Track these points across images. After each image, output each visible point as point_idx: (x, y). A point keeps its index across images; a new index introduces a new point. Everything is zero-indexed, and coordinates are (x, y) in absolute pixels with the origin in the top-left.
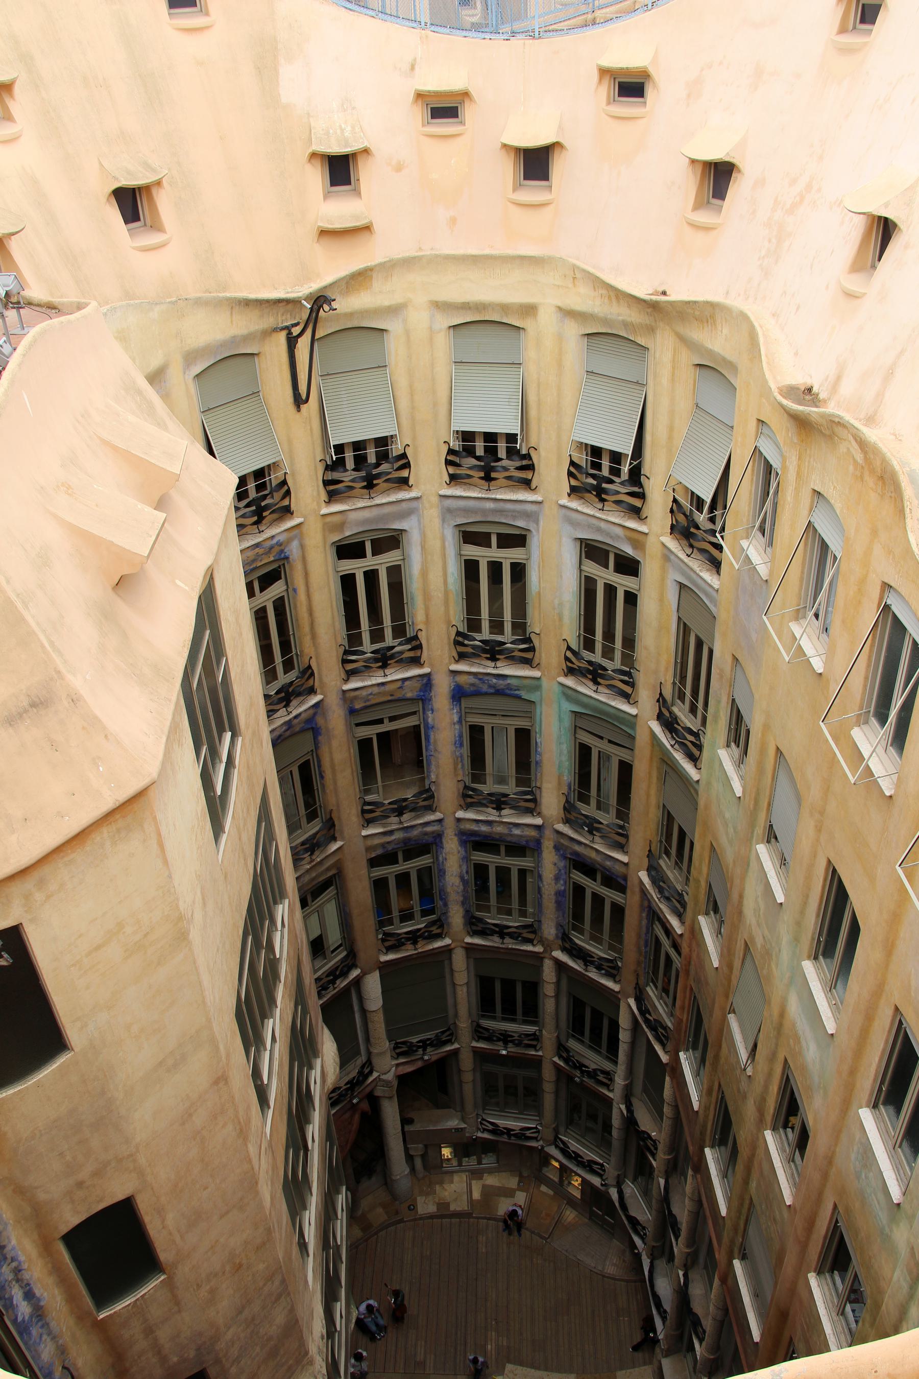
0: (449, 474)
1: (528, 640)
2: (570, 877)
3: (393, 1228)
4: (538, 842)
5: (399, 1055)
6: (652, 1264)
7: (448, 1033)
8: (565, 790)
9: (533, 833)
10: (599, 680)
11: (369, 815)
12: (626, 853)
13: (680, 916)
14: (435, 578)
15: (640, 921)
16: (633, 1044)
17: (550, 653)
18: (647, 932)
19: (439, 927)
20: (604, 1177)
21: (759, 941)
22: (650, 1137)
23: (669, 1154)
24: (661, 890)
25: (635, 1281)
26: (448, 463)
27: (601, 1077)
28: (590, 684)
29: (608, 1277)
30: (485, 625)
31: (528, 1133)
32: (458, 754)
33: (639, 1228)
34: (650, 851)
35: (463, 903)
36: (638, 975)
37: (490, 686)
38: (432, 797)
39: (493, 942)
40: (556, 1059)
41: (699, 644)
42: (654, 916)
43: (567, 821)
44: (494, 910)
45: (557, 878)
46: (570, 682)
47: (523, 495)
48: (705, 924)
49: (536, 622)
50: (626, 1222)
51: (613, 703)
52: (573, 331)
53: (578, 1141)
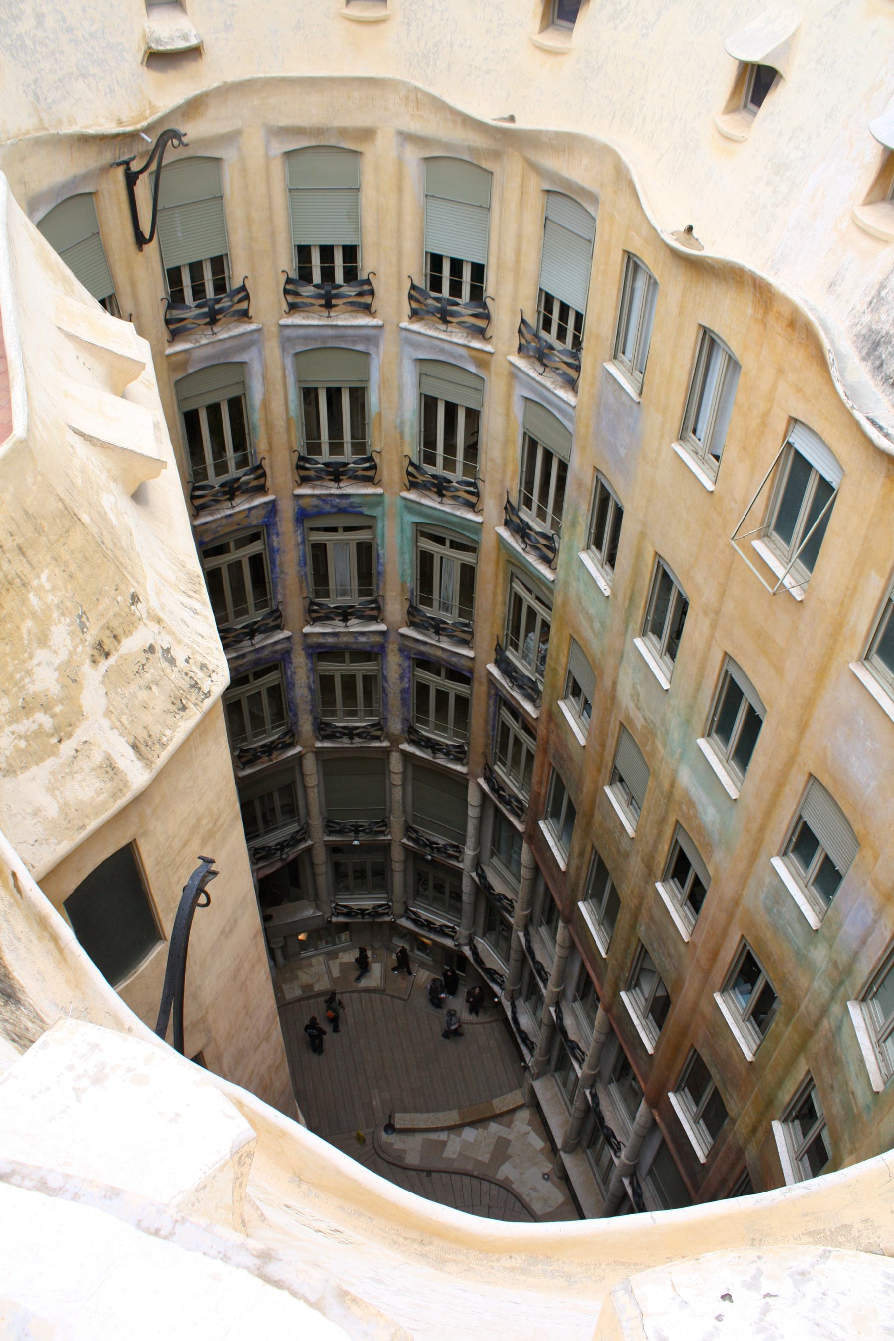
0: (288, 303)
1: (370, 459)
2: (414, 675)
4: (383, 647)
5: (258, 860)
6: (513, 1006)
8: (407, 595)
9: (378, 639)
10: (444, 492)
12: (471, 648)
13: (532, 700)
14: (277, 407)
15: (488, 708)
16: (481, 819)
17: (392, 470)
18: (494, 719)
21: (639, 722)
22: (506, 898)
23: (526, 910)
25: (490, 1022)
26: (286, 292)
28: (435, 497)
30: (325, 448)
31: (380, 910)
32: (303, 573)
33: (496, 976)
34: (498, 644)
35: (312, 712)
37: (333, 506)
39: (344, 743)
40: (405, 841)
41: (548, 456)
42: (503, 701)
43: (412, 624)
44: (340, 714)
45: (402, 678)
46: (412, 495)
47: (363, 320)
48: (568, 710)
49: (376, 441)
50: (483, 974)
51: (458, 513)
52: (412, 156)
53: (426, 910)
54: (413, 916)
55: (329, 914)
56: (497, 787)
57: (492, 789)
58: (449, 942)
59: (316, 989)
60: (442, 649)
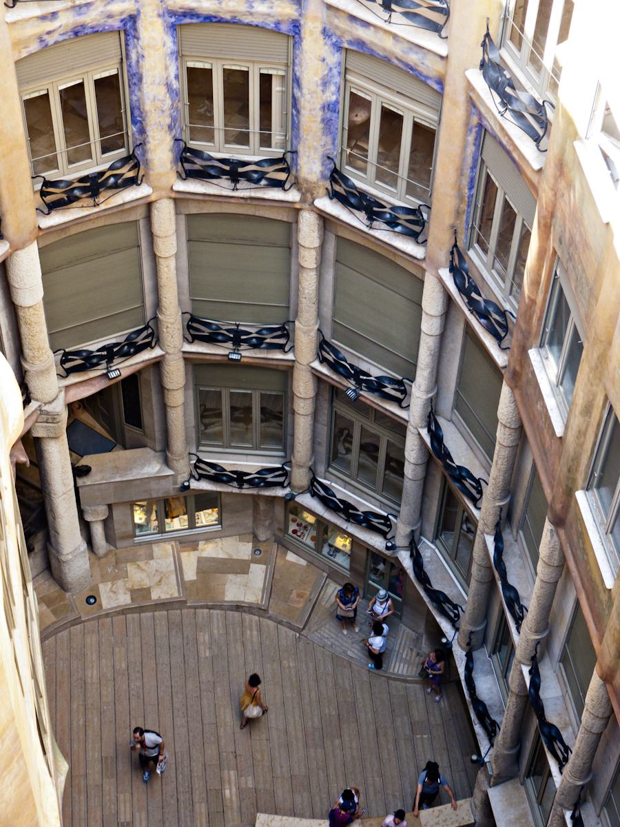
2: (346, 80)
3: (65, 633)
5: (69, 372)
6: (469, 657)
7: (145, 334)
16: (442, 338)
18: (473, 168)
19: (134, 166)
20: (389, 536)
23: (502, 499)
24: (507, 100)
27: (389, 390)
29: (395, 679)
33: (447, 607)
34: (487, 35)
35: (170, 128)
36: (455, 232)
39: (221, 187)
44: (219, 136)
45: (325, 84)
53: (346, 484)
54: (322, 493)
55: (186, 476)
56: (468, 286)
57: (461, 289)
58: (377, 542)
59: (155, 595)
60: (395, 36)
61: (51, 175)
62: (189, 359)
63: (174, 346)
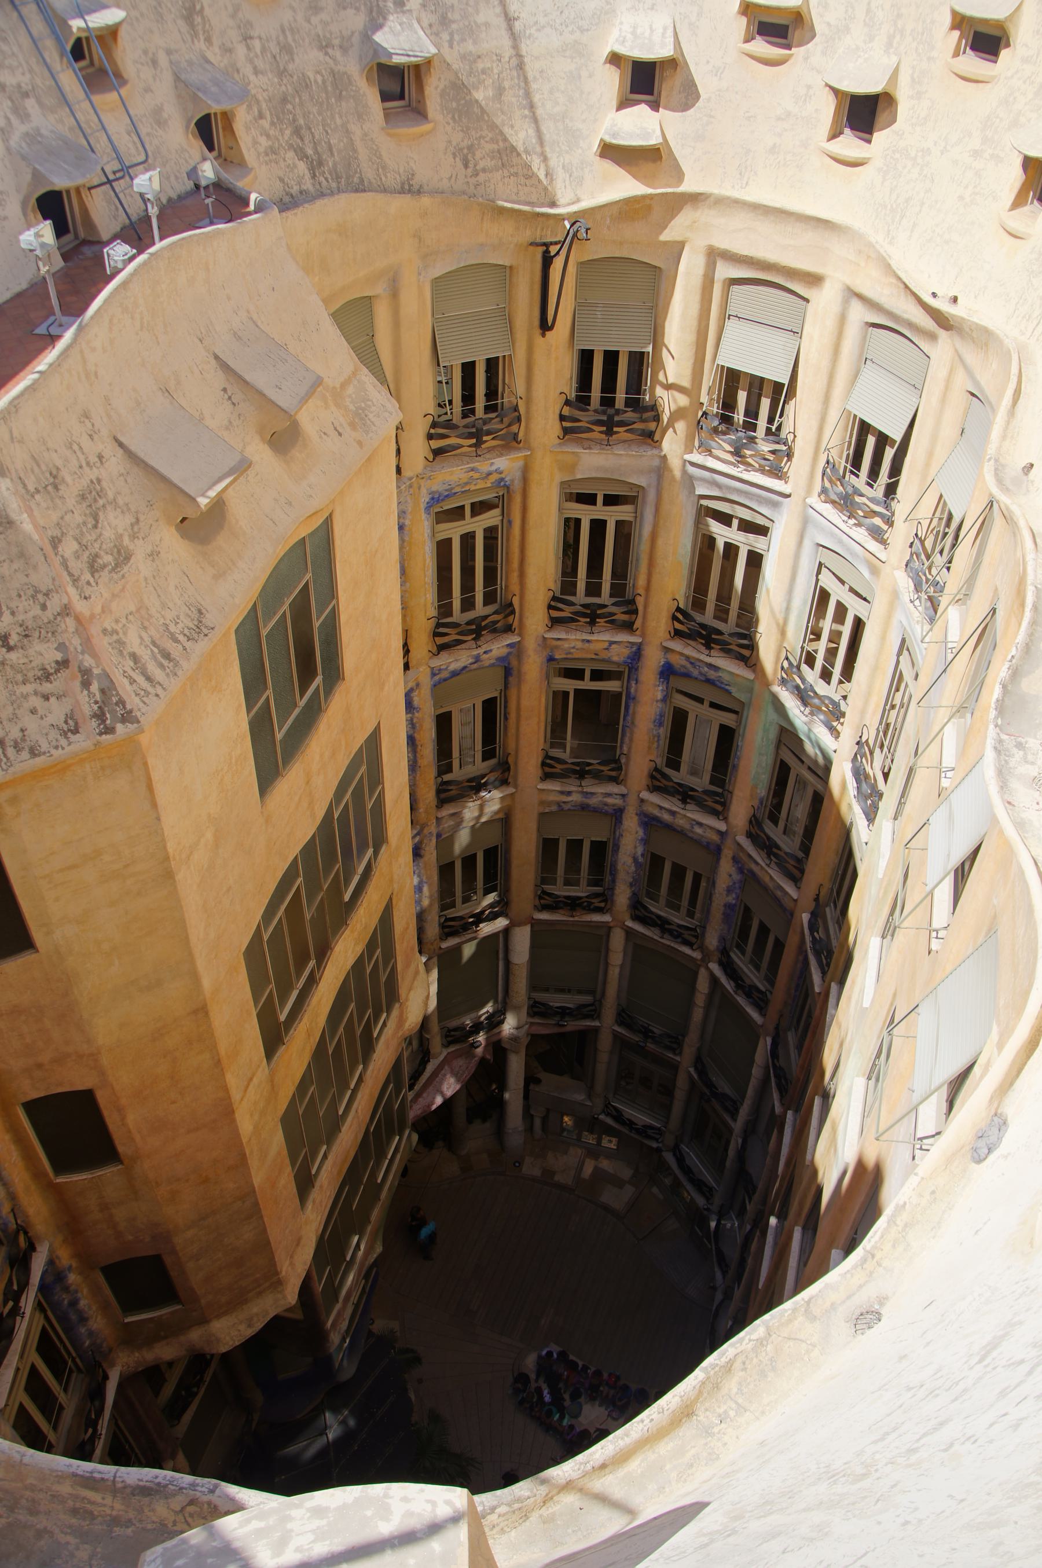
8: (756, 803)
9: (715, 838)
11: (549, 769)
19: (604, 901)
31: (650, 1132)
36: (781, 1016)
37: (701, 673)
38: (620, 769)
40: (692, 1070)
44: (662, 901)
45: (729, 890)
59: (557, 1178)
61: (548, 888)
62: (616, 1035)
63: (607, 1023)
